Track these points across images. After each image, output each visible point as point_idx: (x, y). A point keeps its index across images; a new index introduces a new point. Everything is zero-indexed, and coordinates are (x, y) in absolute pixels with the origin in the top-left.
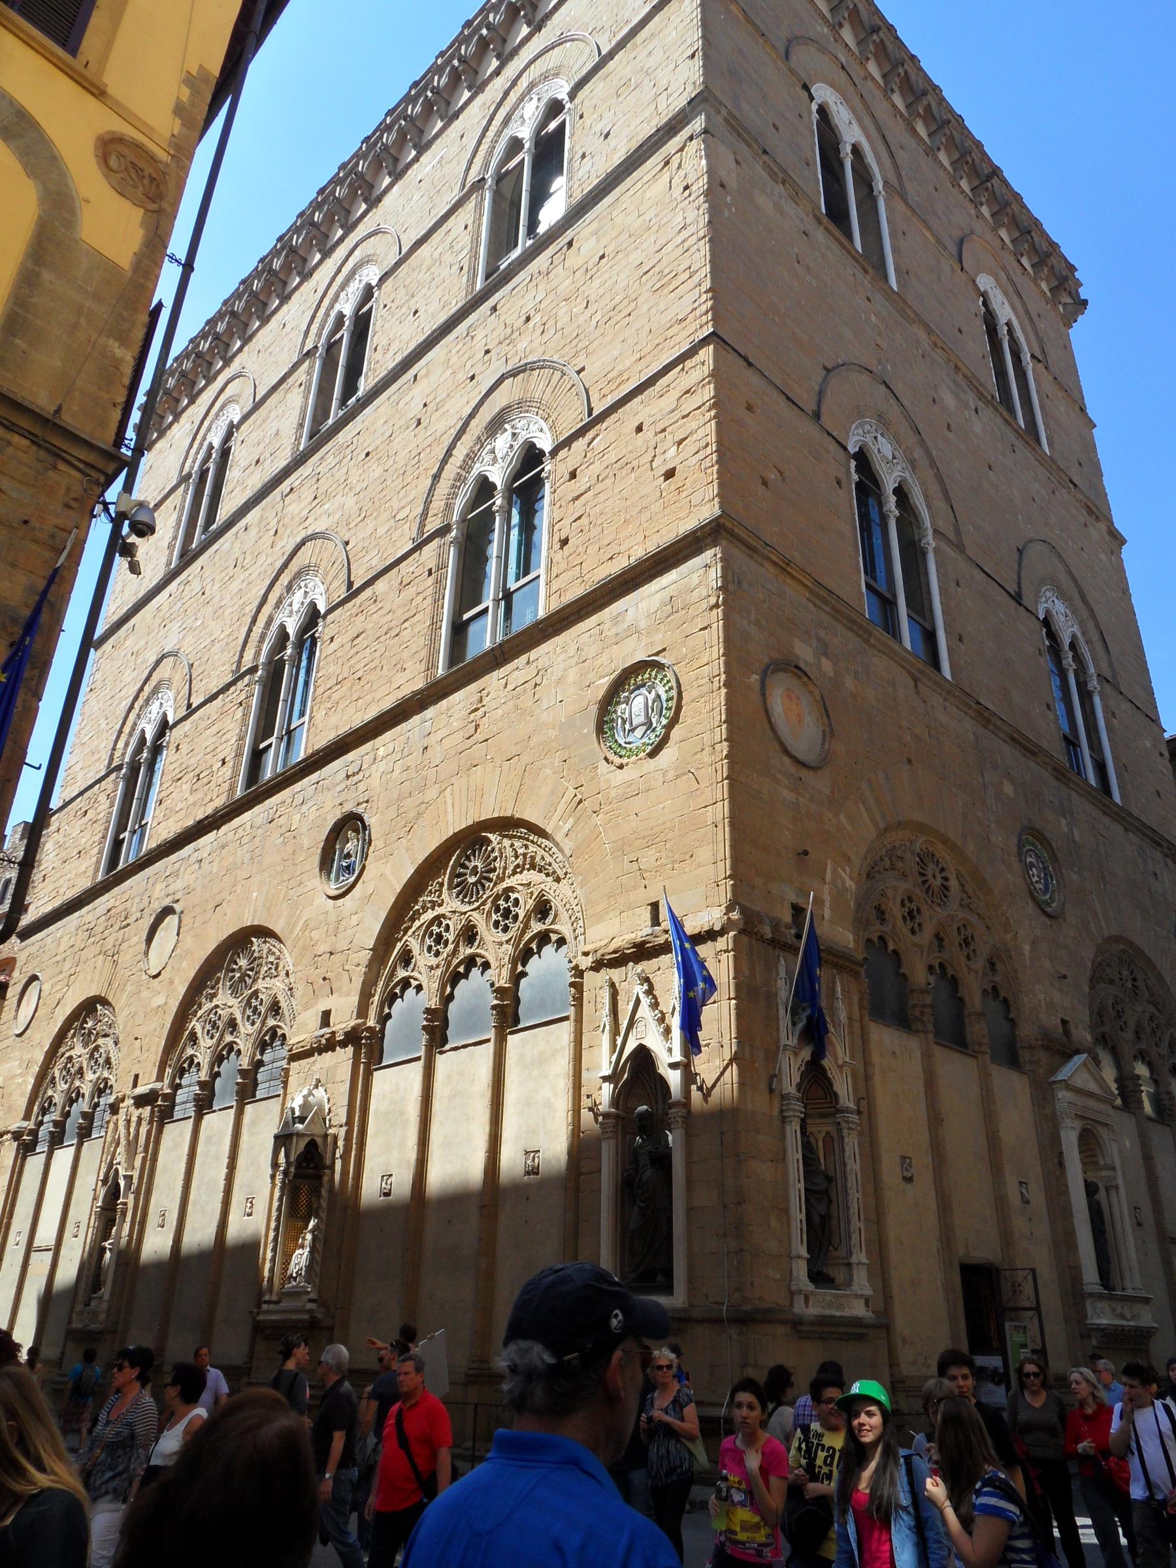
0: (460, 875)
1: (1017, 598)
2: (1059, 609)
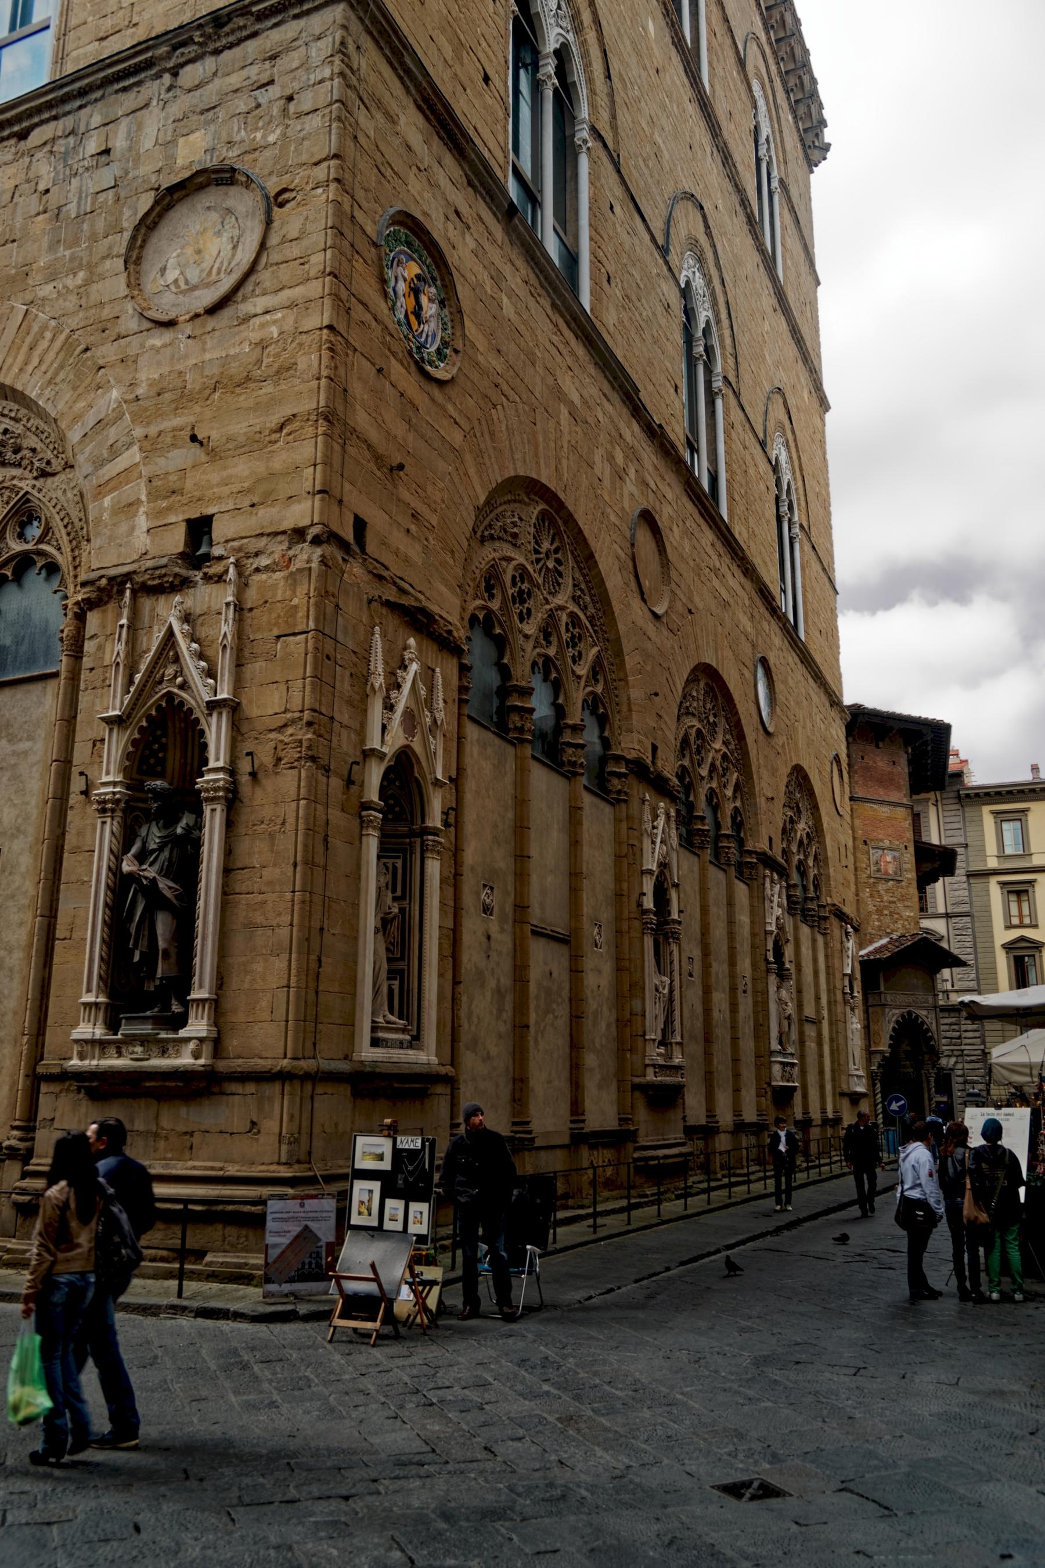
1: (664, 251)
2: (698, 283)
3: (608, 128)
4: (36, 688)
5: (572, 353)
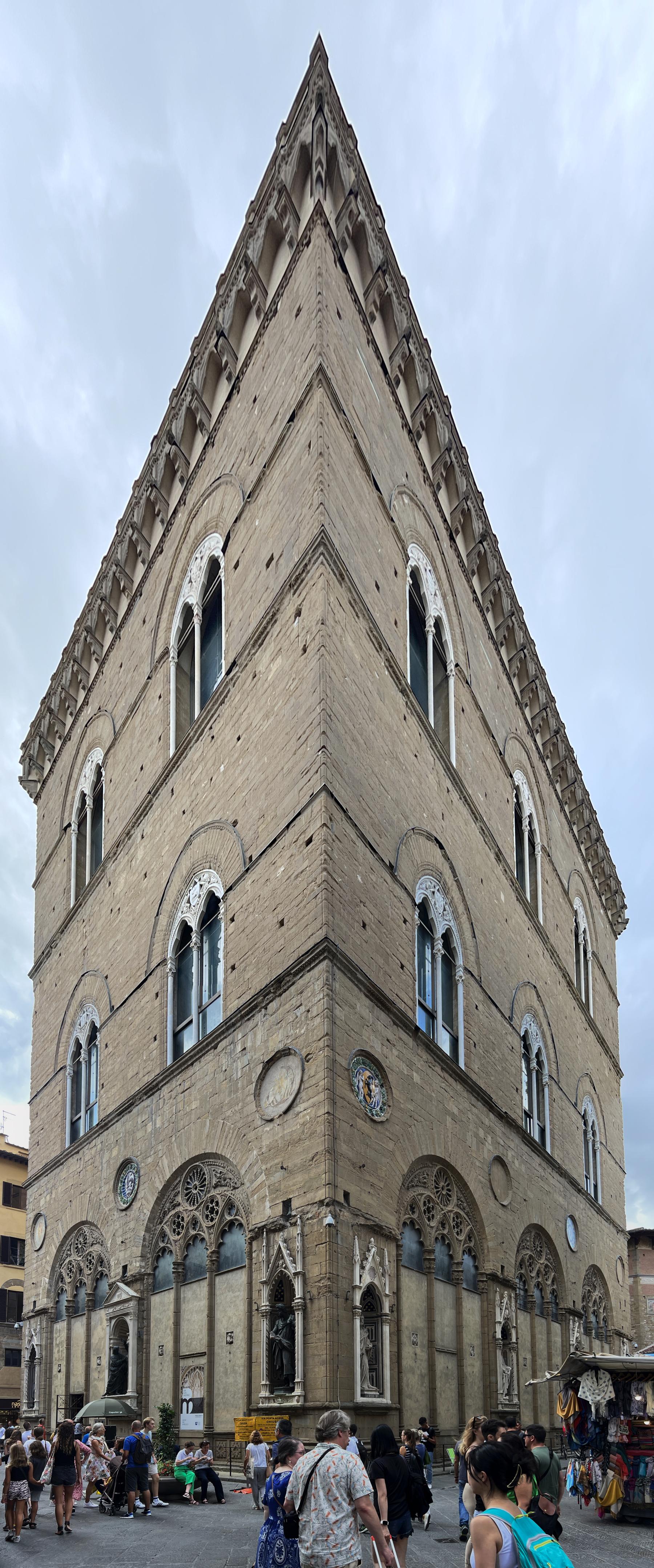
0: (187, 1189)
3: (474, 965)
4: (239, 1272)
5: (454, 1089)
